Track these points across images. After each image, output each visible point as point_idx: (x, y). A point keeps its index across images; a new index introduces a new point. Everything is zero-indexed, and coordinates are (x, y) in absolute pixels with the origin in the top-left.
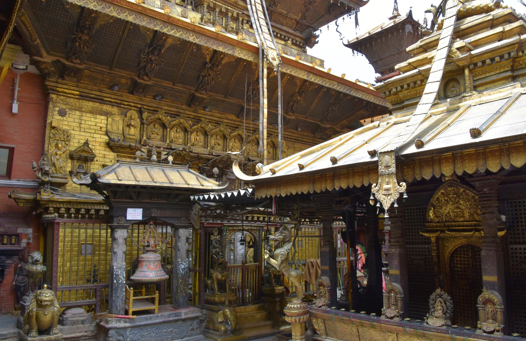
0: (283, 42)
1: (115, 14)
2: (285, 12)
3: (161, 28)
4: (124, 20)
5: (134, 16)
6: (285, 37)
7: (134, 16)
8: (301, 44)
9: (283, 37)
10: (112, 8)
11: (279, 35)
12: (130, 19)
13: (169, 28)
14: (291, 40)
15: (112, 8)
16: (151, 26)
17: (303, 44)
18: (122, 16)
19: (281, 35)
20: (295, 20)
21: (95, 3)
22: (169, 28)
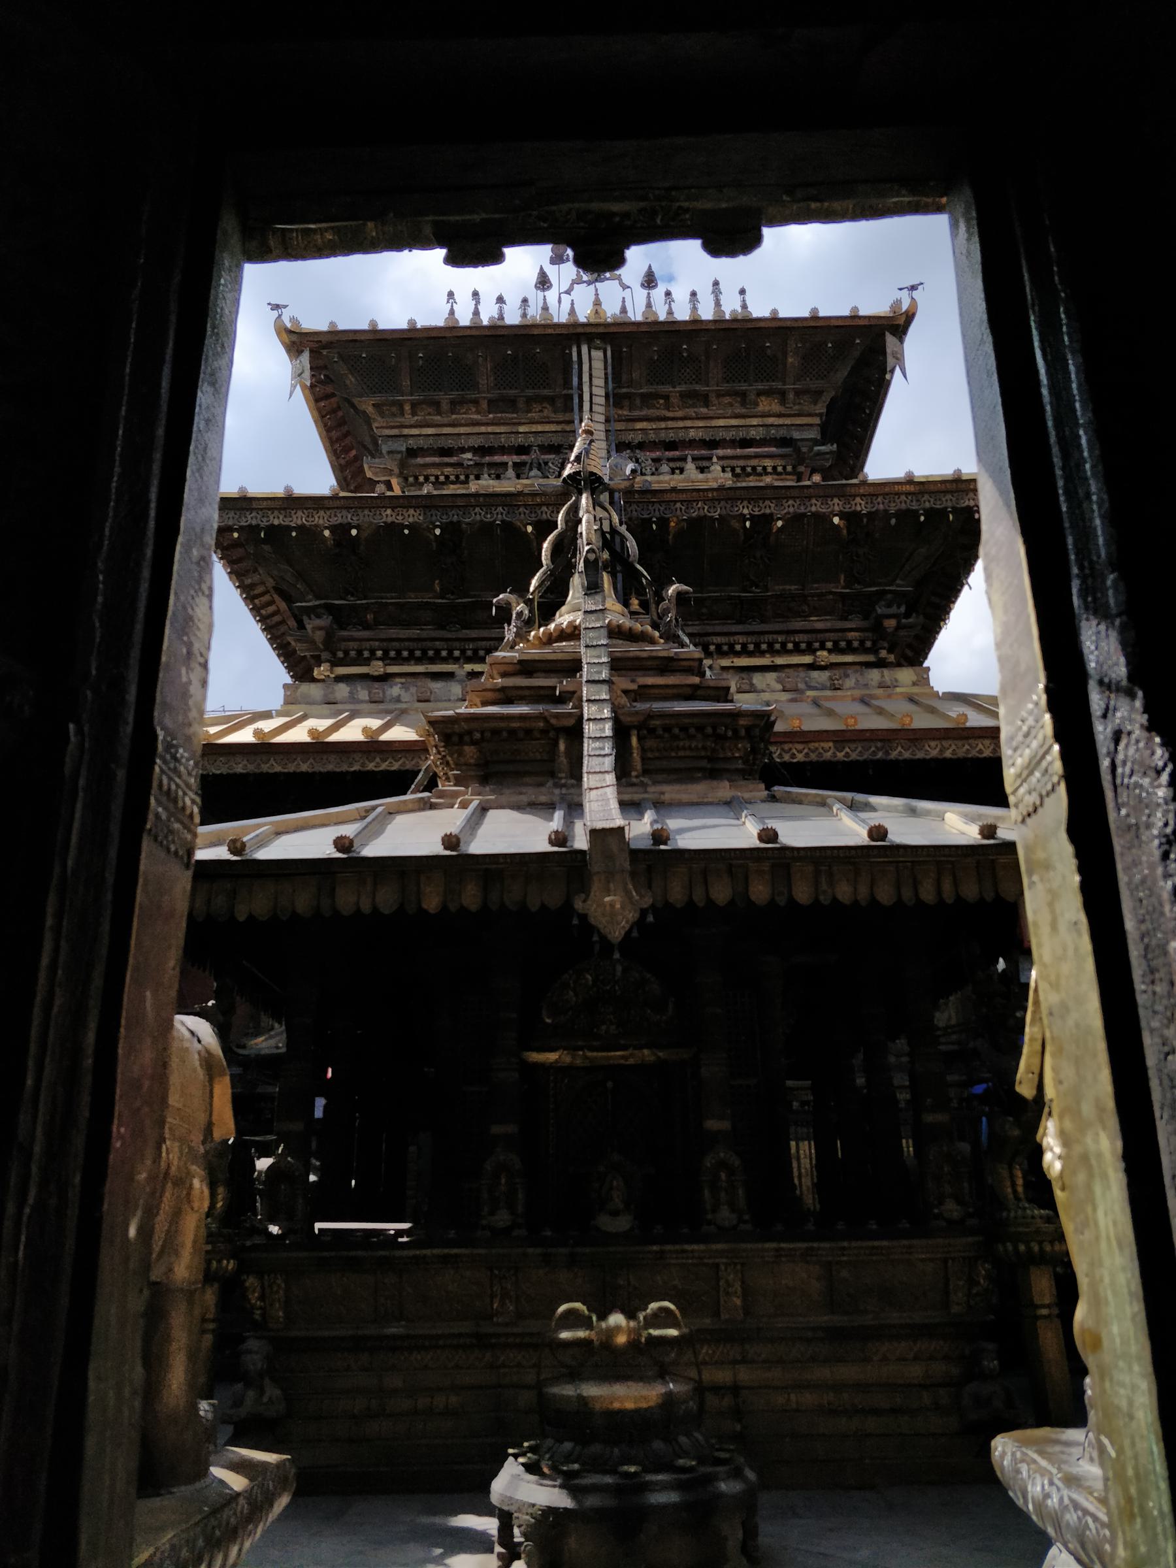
0: (807, 659)
1: (278, 769)
2: (793, 587)
3: (363, 765)
4: (294, 773)
5: (311, 760)
6: (809, 644)
7: (311, 760)
8: (868, 644)
9: (803, 646)
10: (272, 761)
11: (790, 646)
12: (304, 768)
13: (378, 760)
14: (829, 645)
15: (272, 761)
16: (344, 768)
17: (874, 643)
18: (291, 768)
19: (796, 645)
20: (831, 593)
21: (245, 762)
22: (378, 760)
